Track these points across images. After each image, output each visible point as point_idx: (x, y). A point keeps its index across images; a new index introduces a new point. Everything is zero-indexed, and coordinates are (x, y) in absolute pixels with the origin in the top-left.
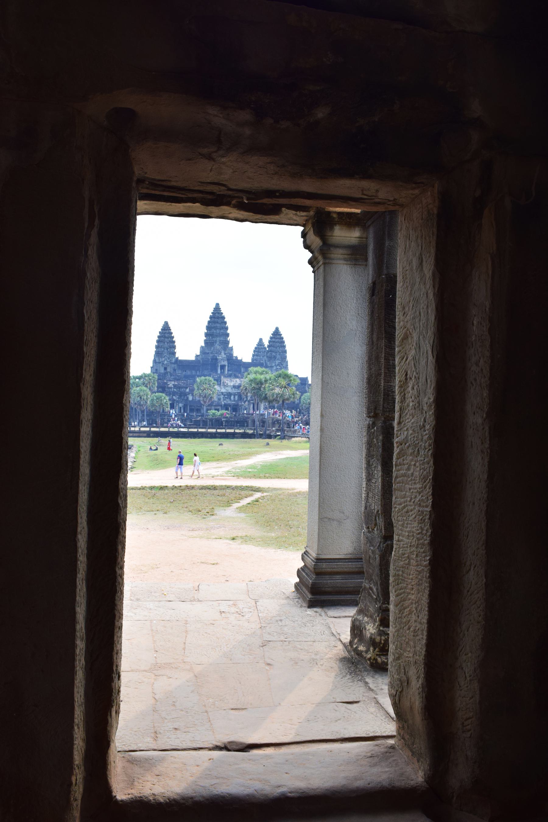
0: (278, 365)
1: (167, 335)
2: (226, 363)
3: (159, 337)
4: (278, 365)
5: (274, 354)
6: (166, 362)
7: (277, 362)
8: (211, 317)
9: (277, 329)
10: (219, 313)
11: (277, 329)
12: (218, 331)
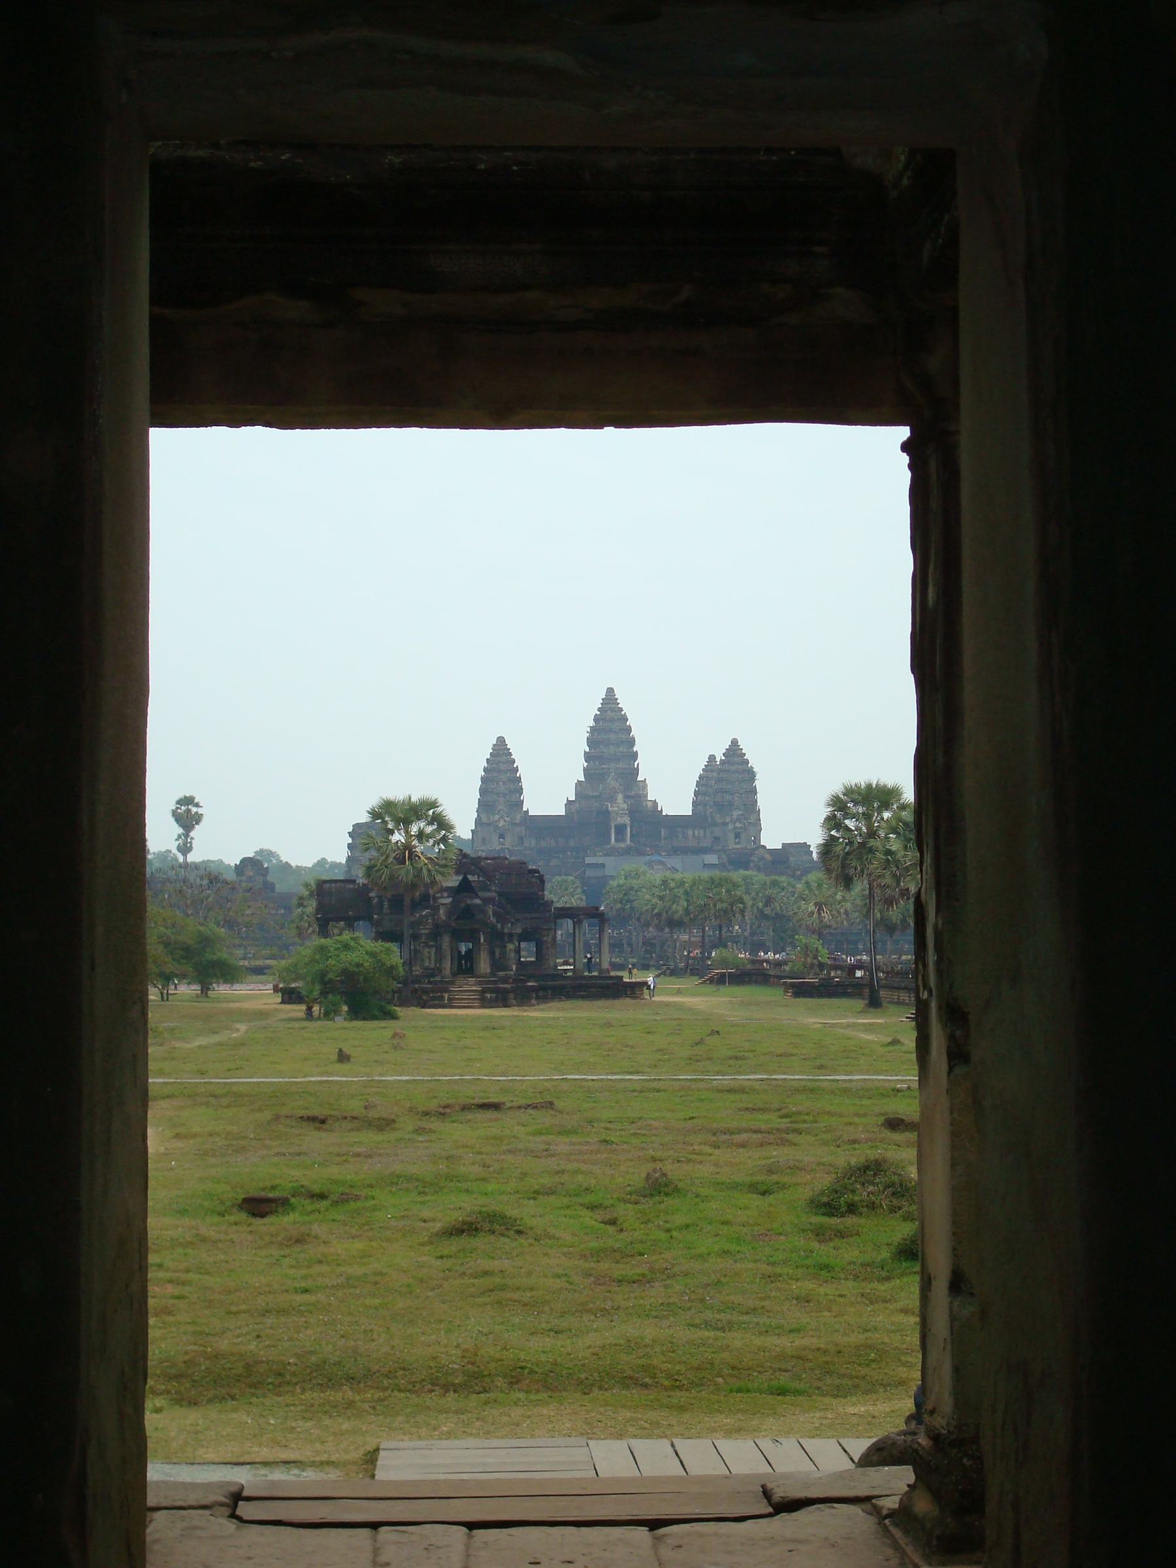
0: (738, 820)
1: (502, 767)
2: (626, 820)
3: (485, 770)
4: (738, 820)
5: (728, 797)
6: (501, 823)
7: (735, 814)
8: (596, 719)
9: (735, 743)
10: (612, 710)
11: (735, 743)
12: (612, 750)
